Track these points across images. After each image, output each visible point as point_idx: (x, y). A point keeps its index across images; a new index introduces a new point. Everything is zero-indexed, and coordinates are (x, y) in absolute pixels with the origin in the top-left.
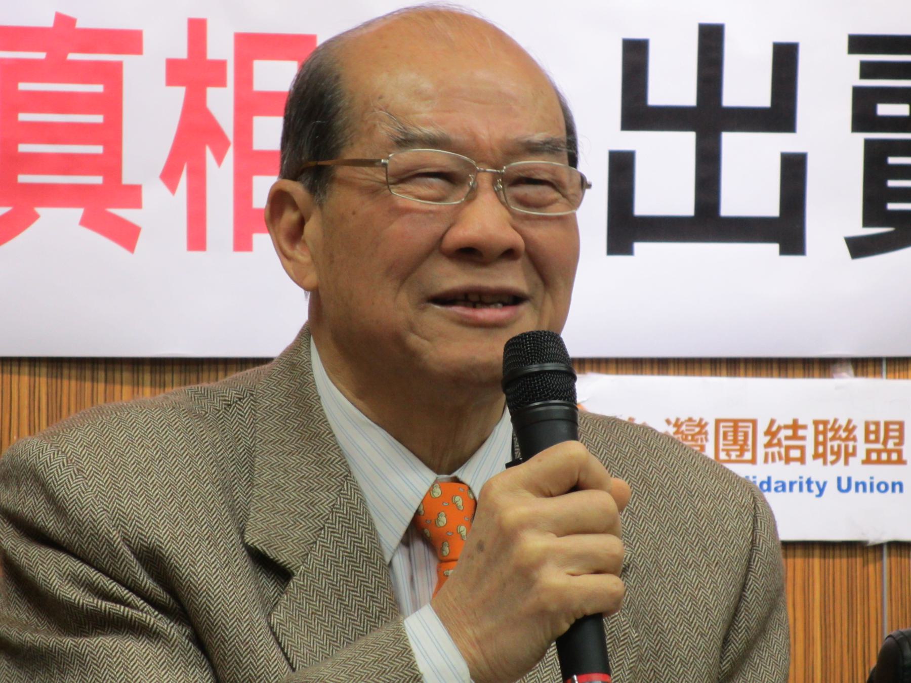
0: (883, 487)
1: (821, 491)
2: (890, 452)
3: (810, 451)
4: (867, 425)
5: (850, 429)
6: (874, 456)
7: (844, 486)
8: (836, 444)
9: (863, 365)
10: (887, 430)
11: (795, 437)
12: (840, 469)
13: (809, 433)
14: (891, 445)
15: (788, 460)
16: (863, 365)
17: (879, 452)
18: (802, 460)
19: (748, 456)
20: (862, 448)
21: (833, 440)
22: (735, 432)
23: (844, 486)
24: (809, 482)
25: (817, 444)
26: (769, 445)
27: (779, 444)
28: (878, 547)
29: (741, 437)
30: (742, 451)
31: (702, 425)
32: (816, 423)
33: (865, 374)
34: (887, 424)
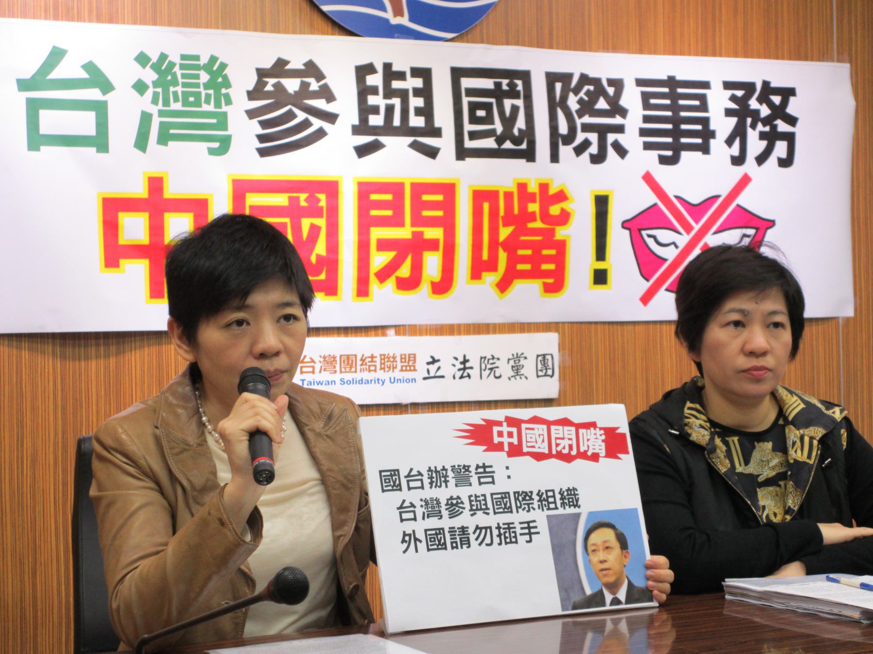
0: (408, 381)
3: (378, 367)
5: (394, 358)
8: (389, 364)
9: (400, 329)
11: (372, 361)
12: (391, 374)
13: (378, 360)
14: (411, 363)
15: (370, 371)
16: (400, 329)
18: (375, 371)
19: (353, 370)
20: (399, 365)
26: (362, 365)
30: (351, 367)
31: (334, 357)
32: (381, 355)
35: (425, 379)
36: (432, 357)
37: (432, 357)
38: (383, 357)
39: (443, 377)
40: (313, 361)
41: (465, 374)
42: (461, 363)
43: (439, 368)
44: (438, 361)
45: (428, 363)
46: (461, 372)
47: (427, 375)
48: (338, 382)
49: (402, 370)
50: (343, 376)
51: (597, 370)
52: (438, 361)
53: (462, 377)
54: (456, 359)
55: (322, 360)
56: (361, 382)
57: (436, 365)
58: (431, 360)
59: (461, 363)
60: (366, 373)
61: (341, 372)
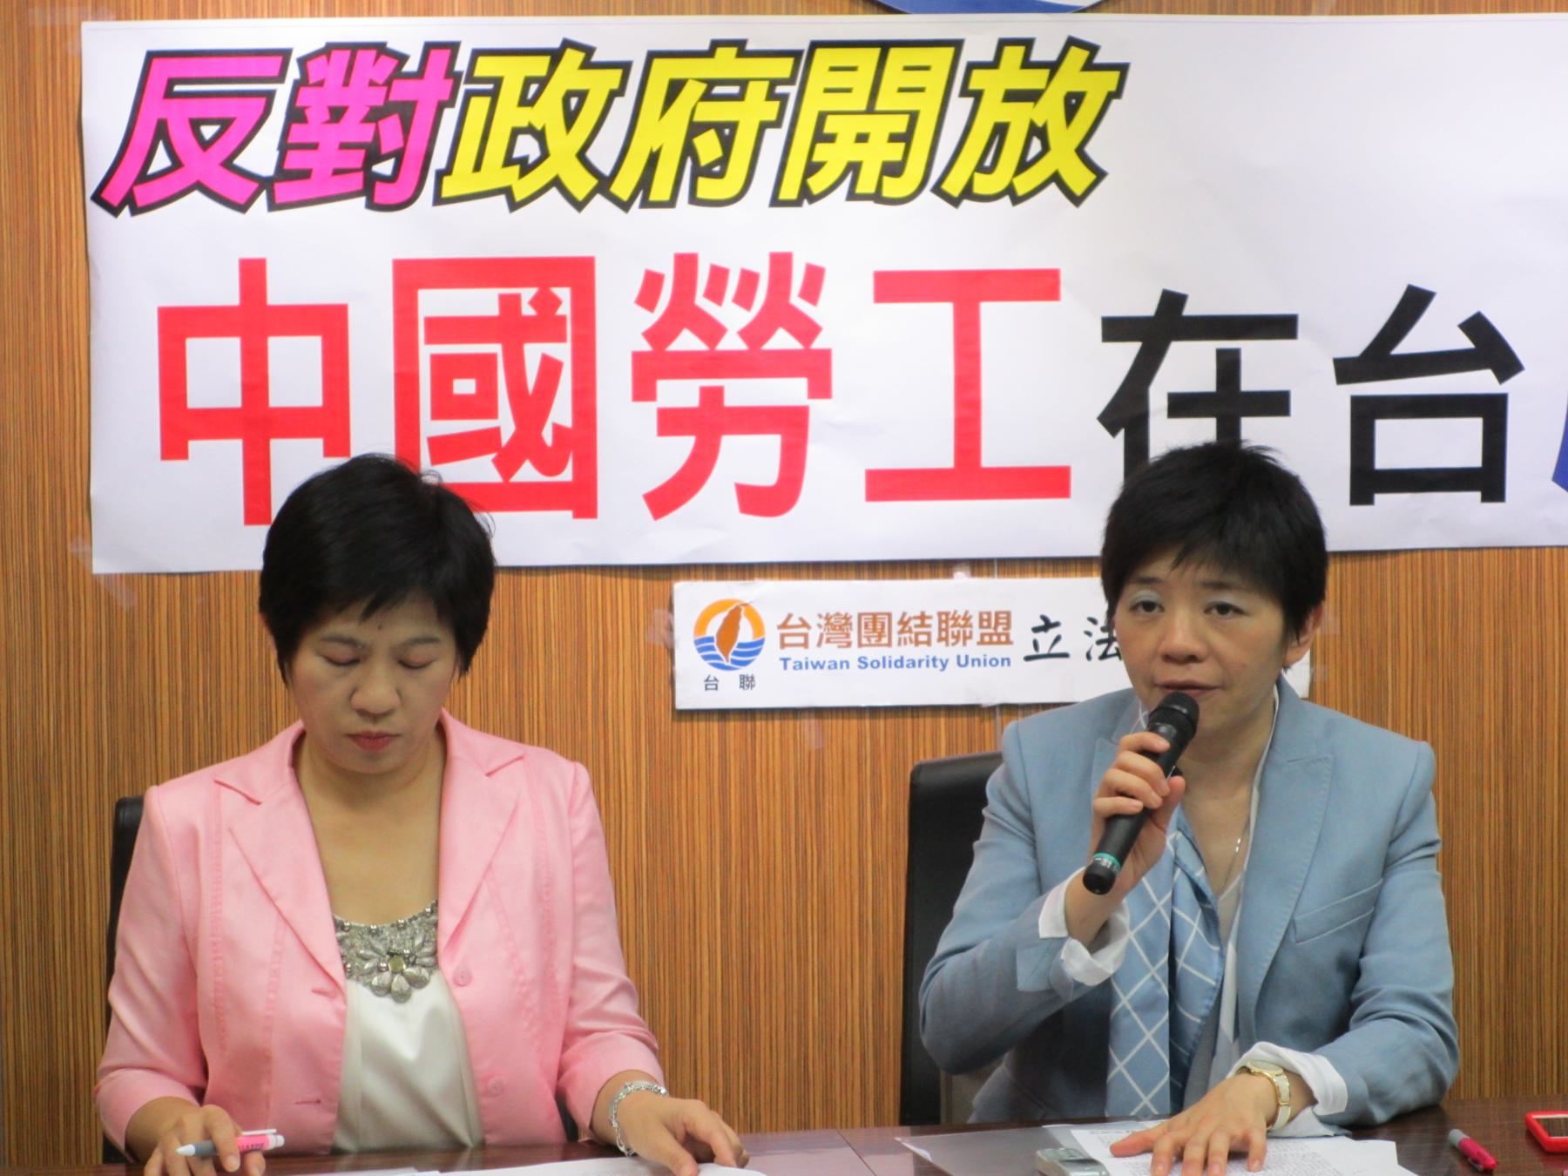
0: (994, 662)
1: (944, 666)
2: (999, 635)
3: (935, 636)
4: (981, 614)
5: (967, 618)
6: (987, 639)
7: (963, 661)
8: (956, 630)
9: (979, 566)
10: (997, 618)
11: (923, 625)
12: (959, 649)
13: (934, 622)
14: (1000, 629)
15: (917, 643)
16: (979, 566)
17: (991, 635)
18: (928, 643)
19: (885, 640)
20: (977, 632)
21: (953, 626)
22: (874, 622)
23: (963, 661)
24: (934, 660)
25: (940, 630)
26: (902, 632)
27: (910, 631)
28: (992, 710)
29: (879, 626)
30: (880, 636)
32: (940, 614)
33: (980, 574)
34: (997, 614)
35: (1028, 658)
36: (1044, 618)
37: (1044, 618)
38: (944, 617)
39: (1065, 655)
40: (805, 624)
41: (1112, 650)
42: (1103, 630)
43: (1058, 639)
44: (1057, 624)
45: (1036, 630)
46: (1104, 646)
47: (1033, 653)
48: (854, 663)
49: (982, 642)
50: (865, 652)
51: (1397, 644)
52: (1057, 624)
53: (1104, 656)
54: (1094, 621)
55: (823, 622)
56: (900, 663)
57: (1053, 633)
58: (1042, 623)
59: (1103, 630)
60: (911, 647)
61: (860, 645)
